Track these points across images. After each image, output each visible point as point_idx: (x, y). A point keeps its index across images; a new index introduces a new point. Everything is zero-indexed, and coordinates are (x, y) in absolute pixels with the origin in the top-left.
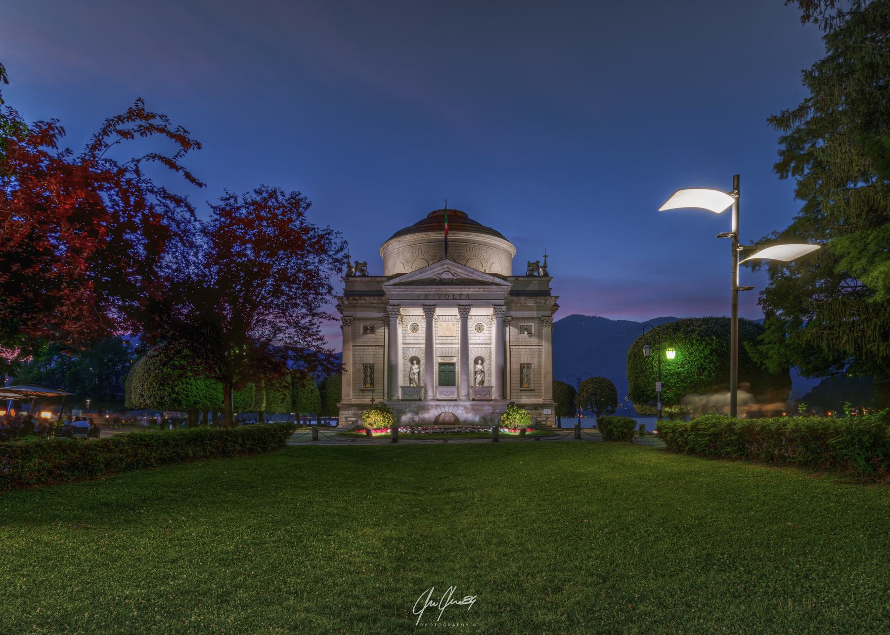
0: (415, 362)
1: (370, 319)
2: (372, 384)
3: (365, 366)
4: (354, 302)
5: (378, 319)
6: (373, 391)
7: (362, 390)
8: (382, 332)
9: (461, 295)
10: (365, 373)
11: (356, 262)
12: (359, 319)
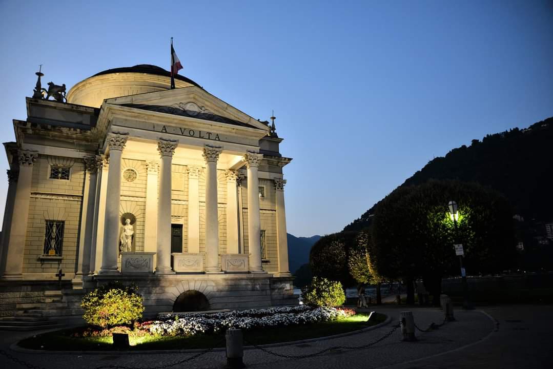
0: (128, 221)
1: (64, 158)
2: (59, 250)
3: (50, 224)
4: (42, 132)
5: (76, 160)
6: (60, 260)
7: (42, 261)
8: (79, 181)
9: (209, 133)
10: (48, 234)
11: (51, 84)
12: (47, 157)
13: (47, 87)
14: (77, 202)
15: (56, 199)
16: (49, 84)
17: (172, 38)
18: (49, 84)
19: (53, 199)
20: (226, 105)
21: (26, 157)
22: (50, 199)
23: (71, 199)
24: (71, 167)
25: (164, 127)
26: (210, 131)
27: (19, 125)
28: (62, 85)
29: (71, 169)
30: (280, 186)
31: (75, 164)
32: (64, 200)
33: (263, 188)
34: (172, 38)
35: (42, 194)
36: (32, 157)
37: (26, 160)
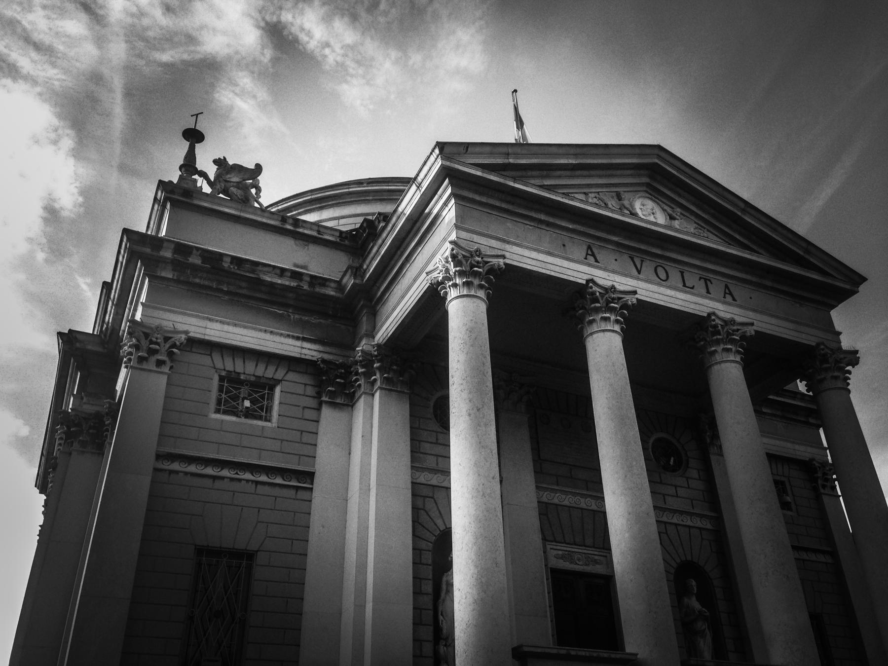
11: (220, 163)
13: (212, 171)
14: (292, 492)
15: (232, 479)
16: (215, 162)
18: (215, 162)
19: (223, 478)
20: (742, 205)
21: (151, 342)
22: (214, 478)
23: (279, 481)
24: (279, 382)
25: (589, 248)
27: (138, 248)
28: (252, 166)
29: (278, 390)
31: (291, 376)
32: (257, 483)
36: (167, 346)
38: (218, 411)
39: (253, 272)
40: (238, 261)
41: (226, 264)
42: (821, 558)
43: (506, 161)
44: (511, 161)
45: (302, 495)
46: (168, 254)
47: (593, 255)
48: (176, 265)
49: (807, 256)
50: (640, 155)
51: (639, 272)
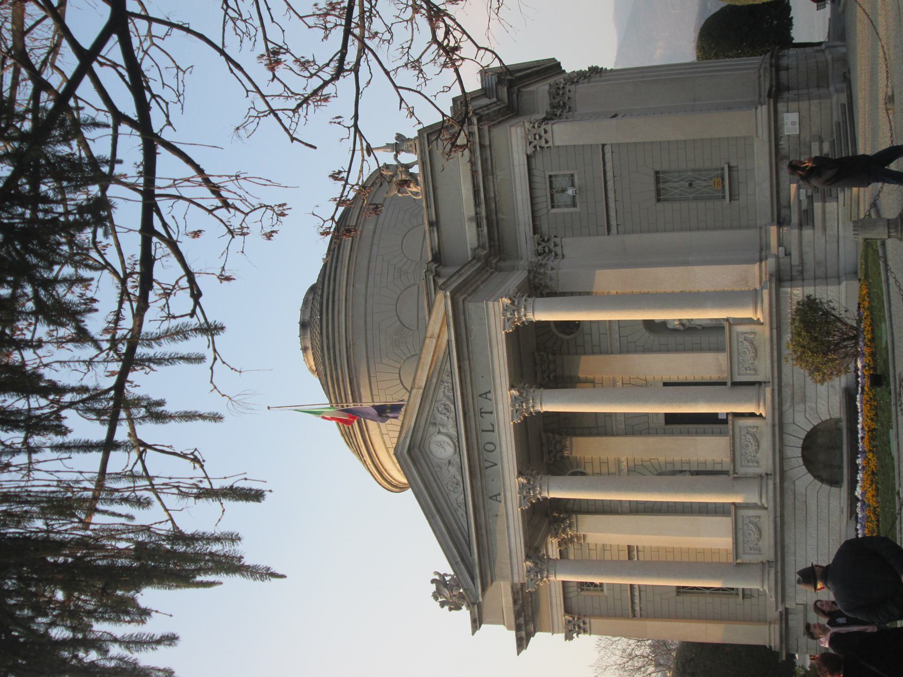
14: (640, 553)
17: (269, 408)
25: (491, 498)
26: (478, 413)
30: (540, 137)
33: (550, 177)
34: (269, 408)
35: (633, 602)
37: (579, 627)
38: (602, 590)
39: (518, 592)
40: (515, 602)
41: (518, 607)
42: (608, 156)
43: (461, 563)
44: (459, 559)
45: (640, 549)
46: (523, 633)
47: (496, 496)
48: (526, 624)
49: (436, 336)
50: (409, 469)
51: (496, 465)
